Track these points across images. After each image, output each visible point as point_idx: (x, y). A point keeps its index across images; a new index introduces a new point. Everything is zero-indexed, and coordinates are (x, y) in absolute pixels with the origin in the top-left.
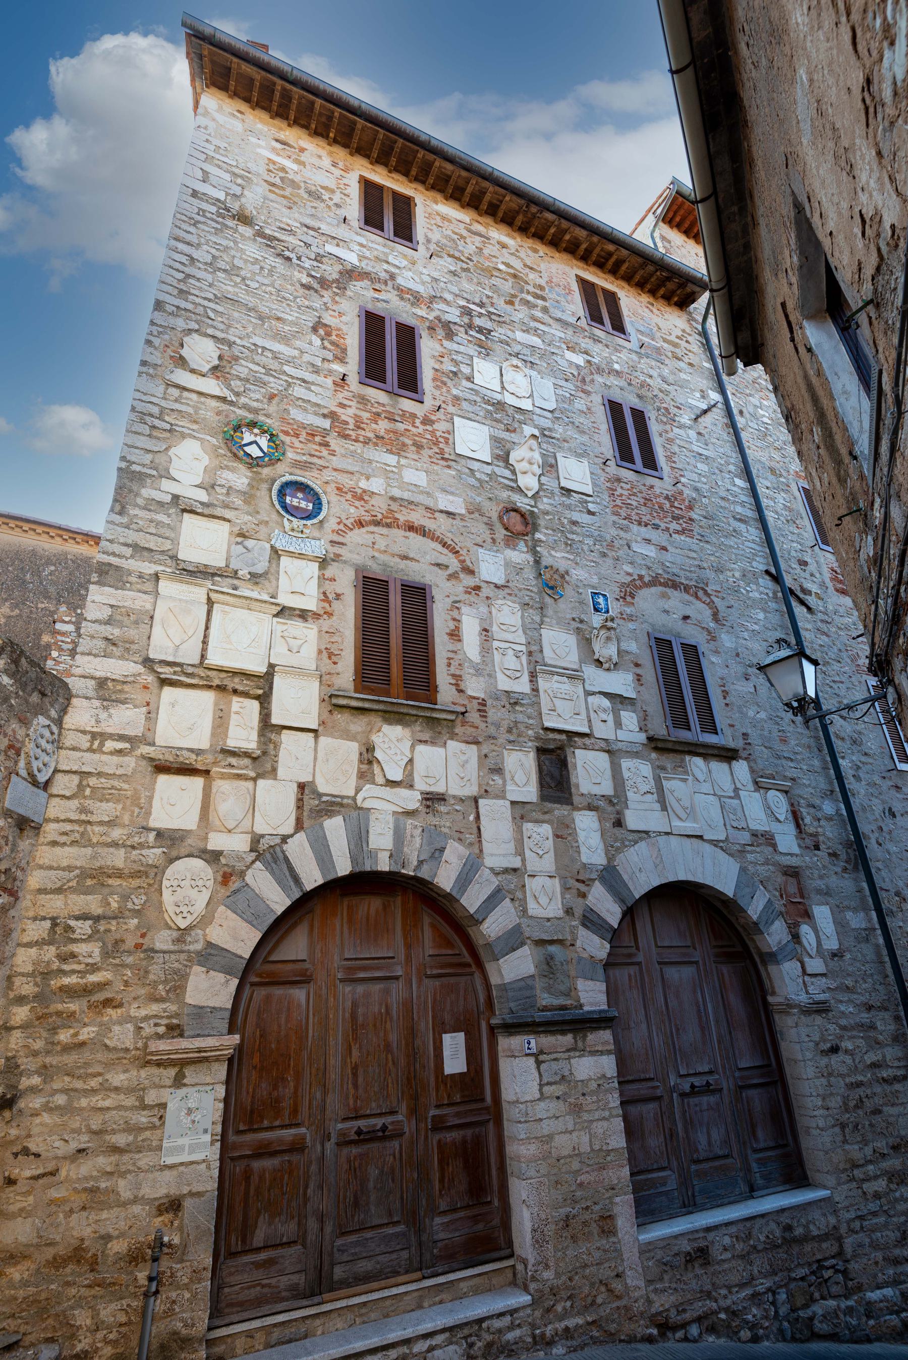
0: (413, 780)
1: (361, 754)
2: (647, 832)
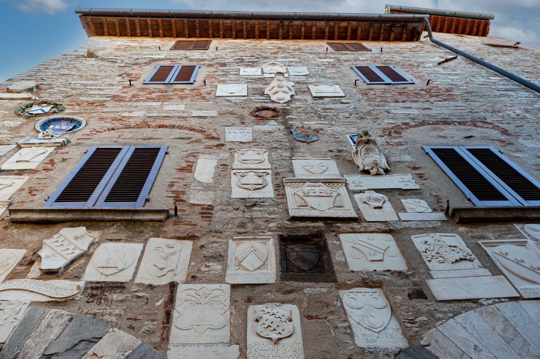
2: (475, 301)
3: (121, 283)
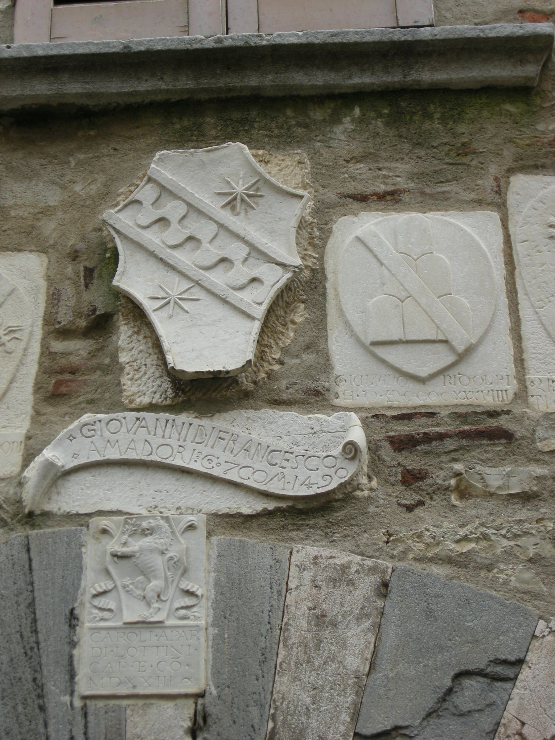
0: (327, 366)
1: (54, 298)
3: (493, 414)
